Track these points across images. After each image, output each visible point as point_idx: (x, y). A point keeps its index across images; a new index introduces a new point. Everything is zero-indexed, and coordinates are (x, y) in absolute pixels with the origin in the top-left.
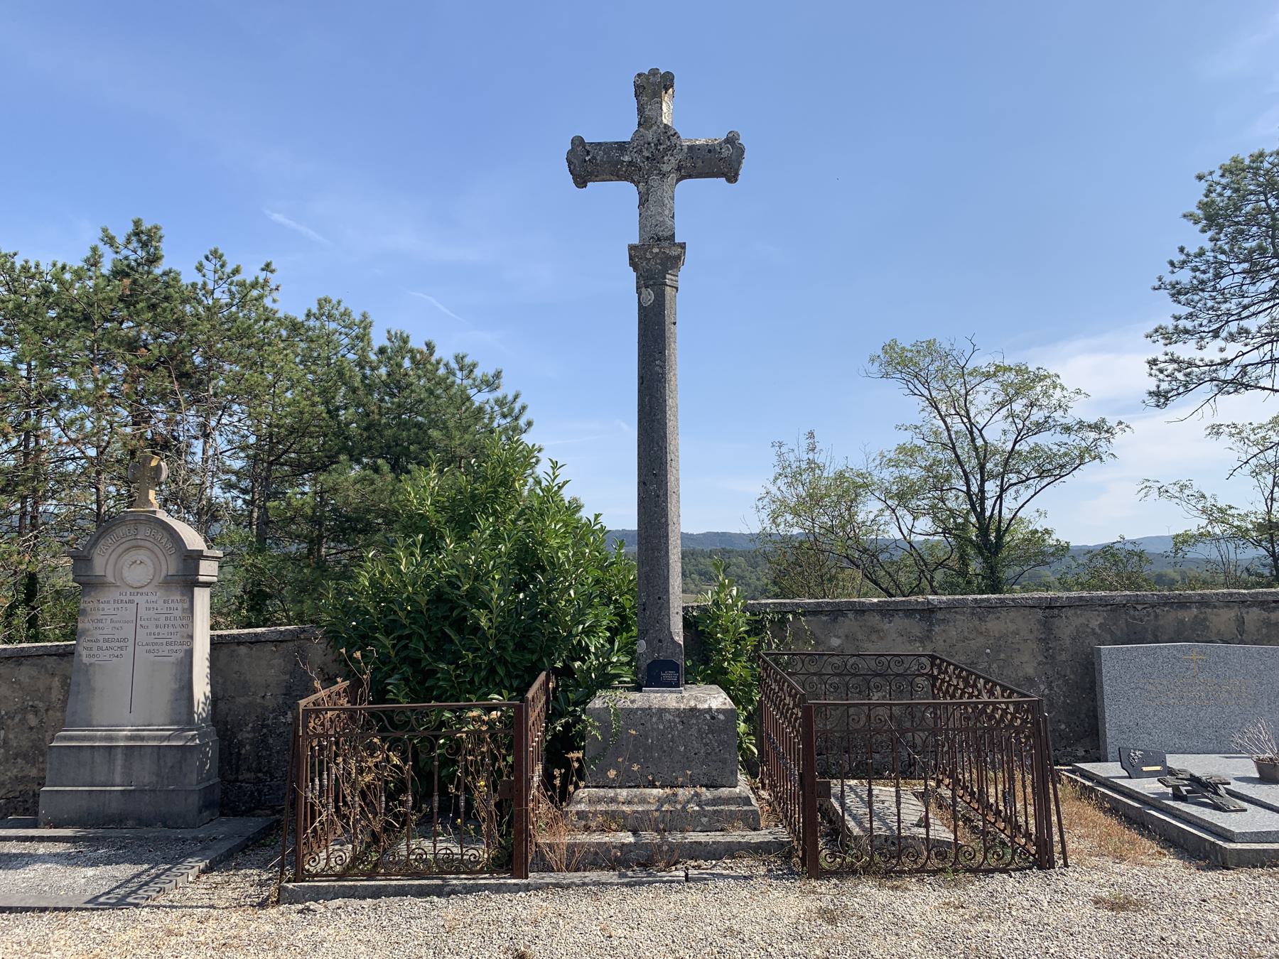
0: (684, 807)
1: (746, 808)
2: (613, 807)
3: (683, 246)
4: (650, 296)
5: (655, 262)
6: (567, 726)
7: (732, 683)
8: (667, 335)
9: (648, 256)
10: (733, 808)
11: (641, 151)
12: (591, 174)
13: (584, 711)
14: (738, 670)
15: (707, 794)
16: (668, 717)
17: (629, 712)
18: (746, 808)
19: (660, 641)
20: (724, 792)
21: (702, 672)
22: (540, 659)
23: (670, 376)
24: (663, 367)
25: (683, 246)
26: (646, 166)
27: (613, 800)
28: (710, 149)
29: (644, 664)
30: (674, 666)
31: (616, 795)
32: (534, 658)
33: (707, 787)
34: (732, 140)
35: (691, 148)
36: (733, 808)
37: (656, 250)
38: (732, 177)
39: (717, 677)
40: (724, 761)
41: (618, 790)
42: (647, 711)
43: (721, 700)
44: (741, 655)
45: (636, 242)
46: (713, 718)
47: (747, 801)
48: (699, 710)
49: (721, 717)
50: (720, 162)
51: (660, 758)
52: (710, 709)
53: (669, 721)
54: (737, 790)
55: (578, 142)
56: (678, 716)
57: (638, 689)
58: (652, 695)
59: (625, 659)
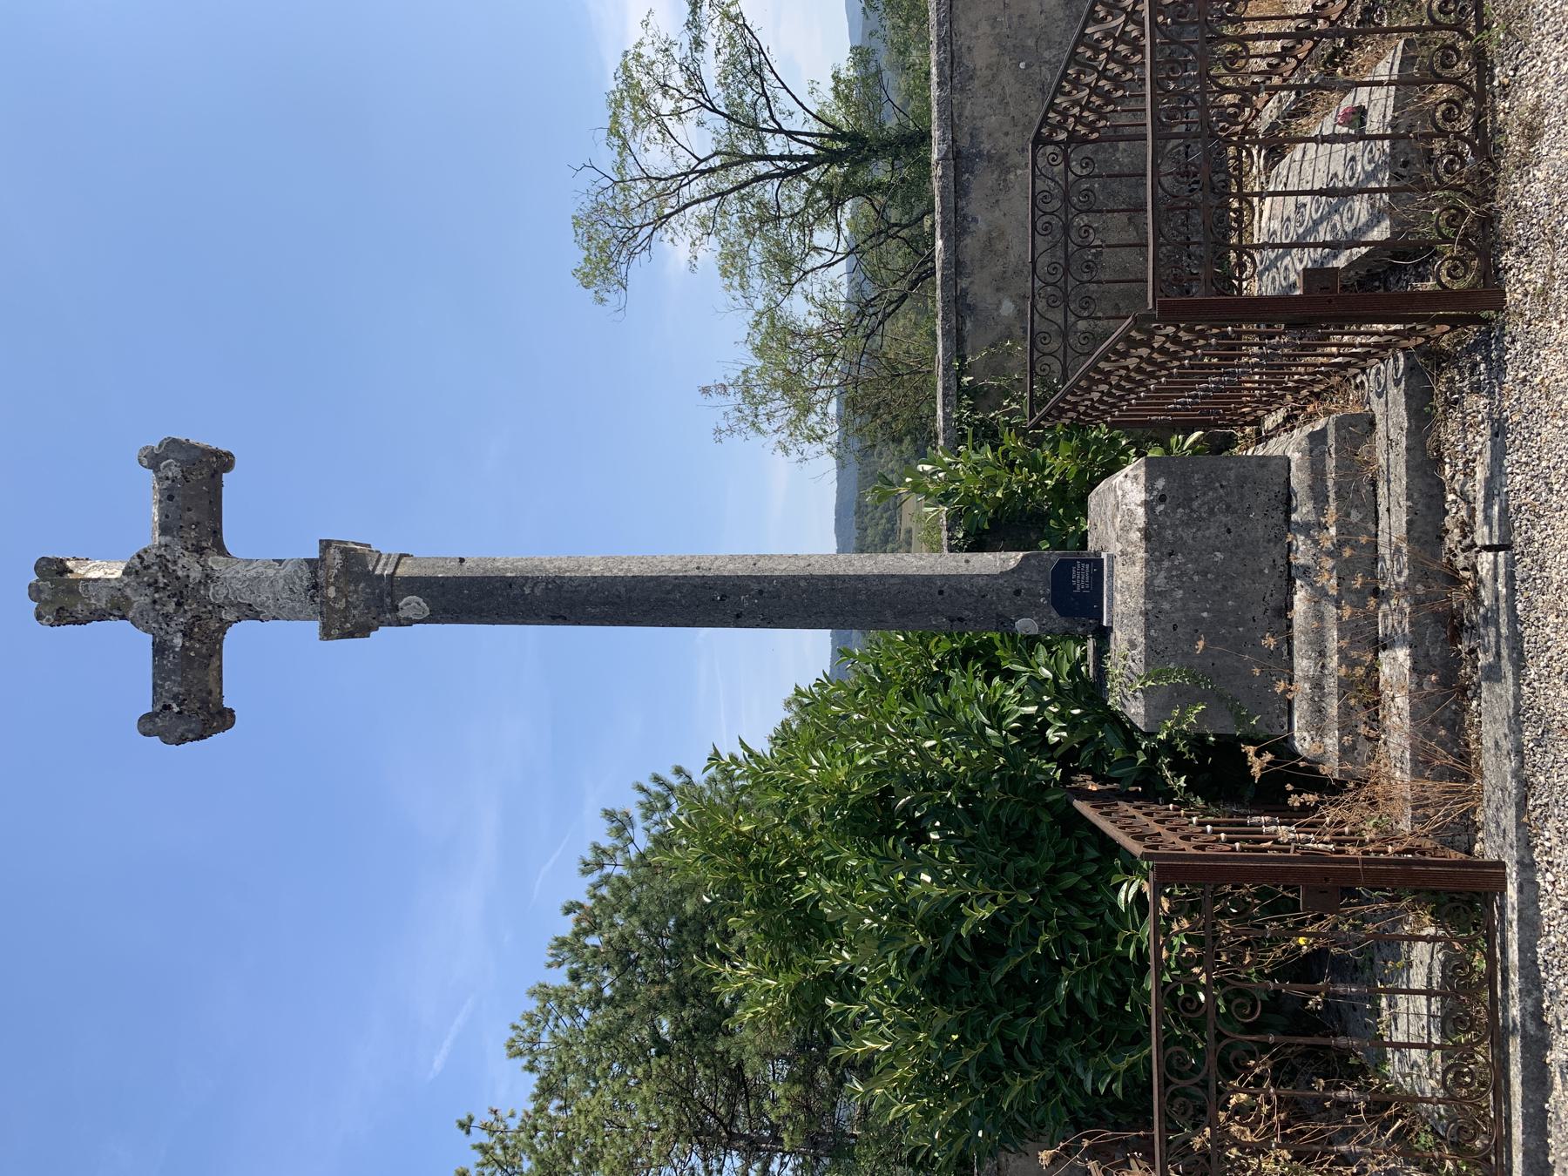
0: (1330, 554)
1: (1331, 440)
2: (1331, 684)
3: (326, 545)
4: (412, 604)
5: (355, 594)
6: (1178, 767)
7: (1081, 472)
8: (479, 573)
9: (342, 605)
10: (1331, 463)
11: (166, 616)
12: (204, 703)
13: (1149, 735)
14: (1061, 463)
15: (1303, 512)
16: (1160, 580)
17: (1154, 652)
18: (1331, 440)
19: (1017, 592)
20: (1299, 479)
21: (1060, 522)
22: (1049, 807)
23: (551, 570)
24: (536, 581)
25: (326, 545)
26: (191, 607)
27: (1318, 685)
28: (168, 497)
29: (1058, 622)
30: (1062, 573)
31: (1306, 678)
32: (1047, 818)
33: (1289, 511)
34: (153, 460)
35: (164, 529)
36: (1331, 463)
37: (332, 592)
38: (224, 461)
39: (1074, 498)
40: (1242, 481)
41: (1298, 673)
42: (1151, 618)
43: (1128, 485)
44: (1034, 457)
45: (315, 626)
46: (1162, 499)
47: (1317, 438)
48: (1148, 523)
49: (1160, 484)
50: (193, 482)
51: (1237, 597)
52: (1146, 503)
53: (1169, 578)
54: (1295, 457)
55: (148, 725)
56: (1159, 561)
57: (1103, 634)
58: (1119, 608)
59: (1042, 655)
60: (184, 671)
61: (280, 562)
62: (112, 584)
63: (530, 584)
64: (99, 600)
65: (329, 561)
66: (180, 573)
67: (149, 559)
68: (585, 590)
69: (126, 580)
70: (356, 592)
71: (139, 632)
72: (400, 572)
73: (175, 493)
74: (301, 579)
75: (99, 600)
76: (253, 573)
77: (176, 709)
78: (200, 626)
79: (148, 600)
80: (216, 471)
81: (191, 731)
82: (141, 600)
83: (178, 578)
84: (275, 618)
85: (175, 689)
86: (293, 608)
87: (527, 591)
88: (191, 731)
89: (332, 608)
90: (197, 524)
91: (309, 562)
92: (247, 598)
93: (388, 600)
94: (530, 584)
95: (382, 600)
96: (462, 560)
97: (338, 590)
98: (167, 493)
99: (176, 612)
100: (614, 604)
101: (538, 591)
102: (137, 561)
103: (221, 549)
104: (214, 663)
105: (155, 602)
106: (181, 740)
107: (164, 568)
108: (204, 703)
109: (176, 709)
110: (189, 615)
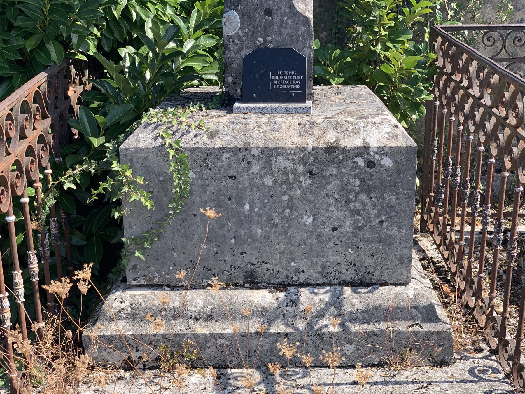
0: (310, 326)
1: (427, 327)
2: (179, 327)
6: (91, 181)
7: (387, 77)
10: (403, 327)
13: (117, 153)
14: (397, 58)
15: (353, 299)
16: (282, 163)
17: (206, 157)
18: (427, 327)
19: (268, 12)
20: (386, 296)
21: (337, 59)
22: (42, 46)
27: (177, 314)
29: (237, 55)
30: (293, 60)
31: (184, 304)
32: (30, 45)
33: (352, 284)
36: (403, 327)
39: (362, 70)
40: (387, 242)
41: (189, 294)
42: (242, 154)
43: (387, 128)
44: (404, 32)
46: (371, 164)
47: (429, 314)
48: (344, 150)
49: (387, 162)
51: (266, 237)
52: (366, 148)
53: (285, 172)
54: (409, 292)
56: (303, 161)
57: (226, 102)
58: (252, 120)
59: (208, 42)
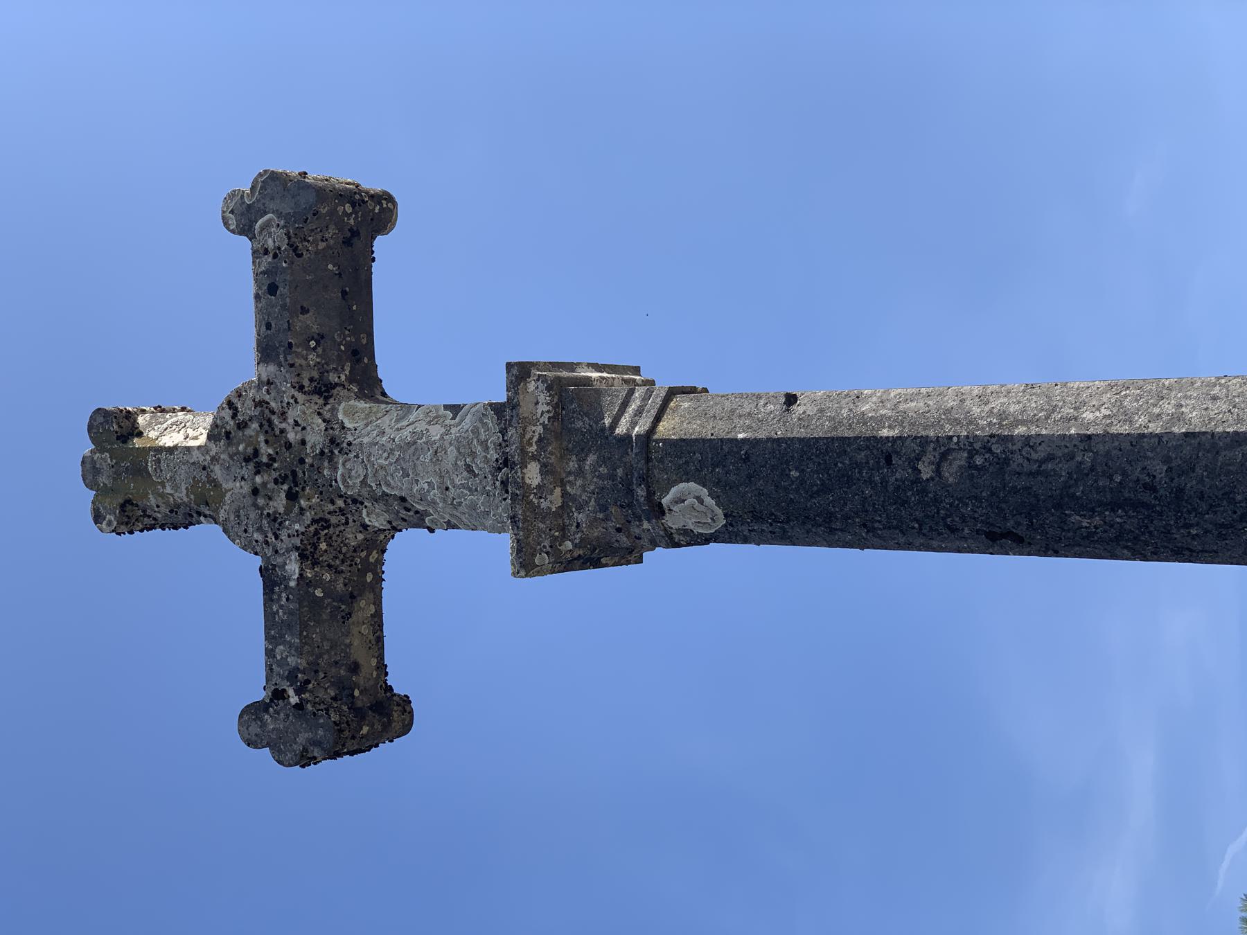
3: (519, 373)
4: (688, 500)
5: (594, 478)
8: (820, 429)
9: (554, 500)
11: (273, 518)
12: (344, 689)
23: (982, 420)
24: (944, 448)
25: (519, 373)
26: (309, 500)
28: (269, 287)
34: (243, 216)
35: (266, 352)
37: (533, 475)
38: (370, 213)
45: (504, 543)
50: (319, 252)
55: (256, 723)
60: (304, 626)
61: (455, 409)
62: (196, 456)
63: (931, 455)
64: (176, 488)
65: (525, 409)
66: (291, 436)
67: (247, 409)
68: (1064, 469)
69: (214, 450)
70: (580, 472)
71: (235, 549)
72: (667, 428)
73: (279, 279)
74: (484, 444)
75: (176, 488)
76: (406, 433)
77: (294, 700)
78: (329, 538)
79: (247, 489)
80: (354, 233)
81: (316, 743)
82: (235, 488)
83: (289, 446)
84: (450, 526)
85: (292, 661)
86: (473, 506)
87: (926, 472)
88: (316, 743)
89: (535, 509)
90: (320, 338)
91: (497, 409)
92: (397, 485)
93: (641, 492)
94: (931, 455)
95: (630, 492)
96: (791, 399)
97: (545, 470)
98: (266, 282)
99: (288, 510)
100: (1137, 505)
101: (950, 473)
102: (227, 414)
103: (368, 384)
104: (364, 608)
105: (255, 492)
106: (305, 760)
107: (267, 426)
108: (344, 689)
109: (294, 700)
110: (308, 516)
